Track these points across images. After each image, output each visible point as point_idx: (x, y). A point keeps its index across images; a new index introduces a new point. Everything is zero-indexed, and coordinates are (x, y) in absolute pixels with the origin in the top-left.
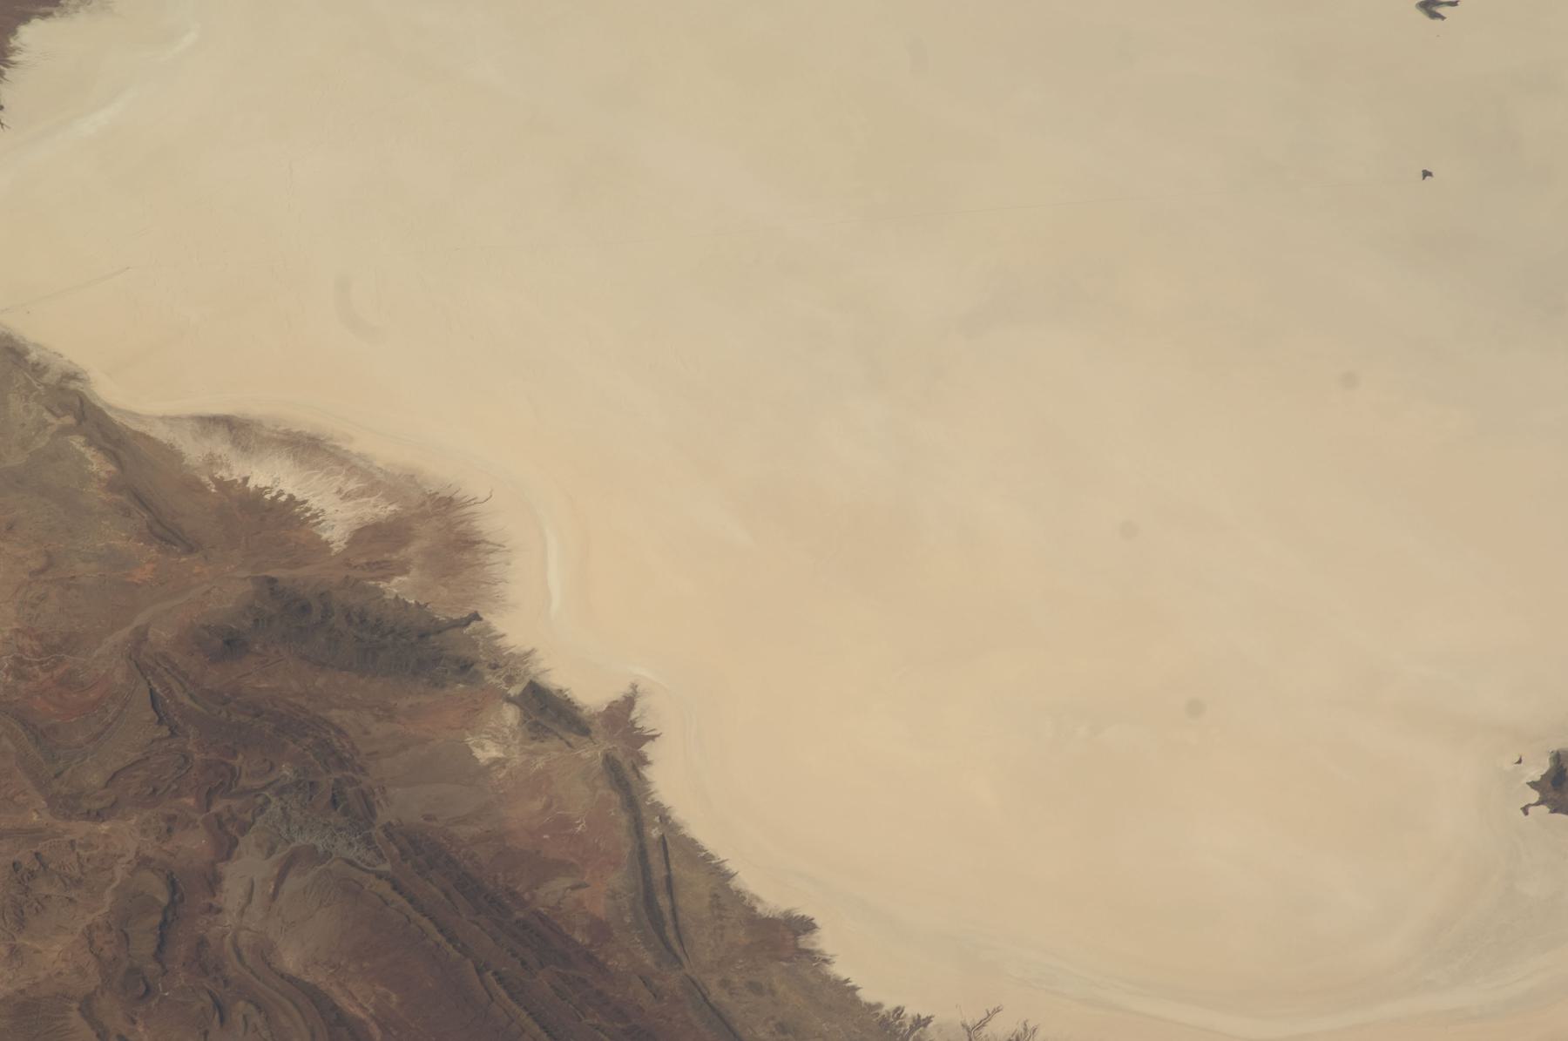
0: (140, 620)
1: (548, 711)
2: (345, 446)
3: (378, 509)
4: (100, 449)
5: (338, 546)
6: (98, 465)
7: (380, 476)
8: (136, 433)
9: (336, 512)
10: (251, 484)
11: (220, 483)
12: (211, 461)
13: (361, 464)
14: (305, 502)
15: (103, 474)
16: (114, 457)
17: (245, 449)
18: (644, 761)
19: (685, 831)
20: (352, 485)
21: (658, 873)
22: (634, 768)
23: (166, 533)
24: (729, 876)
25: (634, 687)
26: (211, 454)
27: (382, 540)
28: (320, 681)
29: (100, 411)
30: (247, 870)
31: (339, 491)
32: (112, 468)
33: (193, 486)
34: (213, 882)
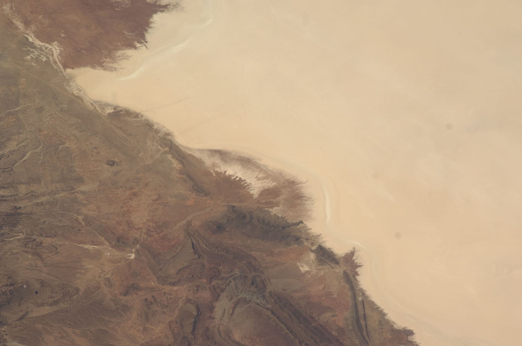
0: (189, 218)
1: (325, 255)
2: (259, 162)
3: (269, 184)
4: (177, 159)
5: (256, 196)
6: (176, 165)
7: (270, 173)
9: (255, 185)
10: (227, 174)
11: (217, 173)
12: (214, 165)
13: (264, 168)
14: (245, 180)
15: (178, 168)
16: (182, 162)
17: (225, 162)
18: (357, 274)
19: (370, 299)
20: (261, 175)
21: (361, 313)
22: (354, 276)
23: (198, 189)
24: (385, 315)
25: (354, 248)
26: (214, 163)
27: (270, 195)
28: (249, 242)
29: (177, 146)
30: (223, 305)
31: (256, 177)
32: (181, 166)
33: (207, 173)
34: (212, 309)
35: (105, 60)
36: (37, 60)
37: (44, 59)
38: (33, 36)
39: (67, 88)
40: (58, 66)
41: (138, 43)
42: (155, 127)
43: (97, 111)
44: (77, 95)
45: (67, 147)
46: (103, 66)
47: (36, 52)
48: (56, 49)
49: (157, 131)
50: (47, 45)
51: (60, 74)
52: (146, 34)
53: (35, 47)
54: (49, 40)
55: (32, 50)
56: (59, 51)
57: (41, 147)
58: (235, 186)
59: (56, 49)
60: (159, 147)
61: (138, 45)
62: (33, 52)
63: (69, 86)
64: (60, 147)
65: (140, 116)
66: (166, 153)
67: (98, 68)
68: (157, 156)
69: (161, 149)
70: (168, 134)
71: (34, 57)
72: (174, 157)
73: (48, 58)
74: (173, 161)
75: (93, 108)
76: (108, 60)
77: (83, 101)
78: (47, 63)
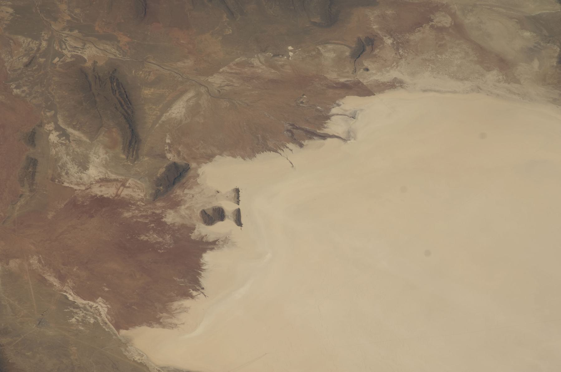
35: (161, 315)
36: (84, 322)
37: (92, 321)
38: (72, 294)
40: (109, 328)
41: (193, 290)
46: (160, 323)
47: (81, 312)
48: (102, 307)
50: (91, 303)
51: (114, 337)
52: (200, 279)
53: (77, 307)
54: (92, 297)
55: (75, 310)
56: (106, 310)
59: (102, 307)
61: (194, 293)
62: (76, 313)
67: (155, 325)
71: (80, 319)
73: (95, 318)
76: (165, 314)
78: (96, 324)
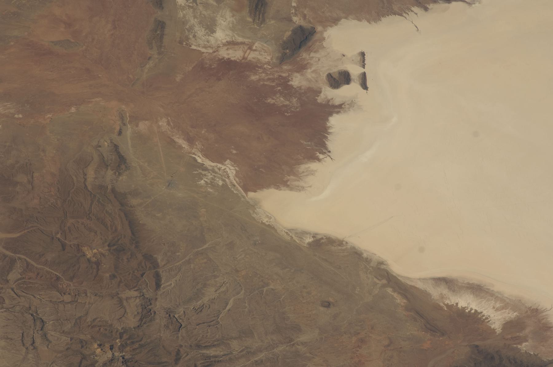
2: (492, 289)
3: (511, 315)
4: (399, 293)
5: (499, 330)
6: (399, 300)
7: (508, 301)
8: (411, 286)
10: (459, 306)
11: (447, 305)
12: (442, 297)
13: (499, 296)
14: (482, 312)
15: (402, 304)
16: (405, 297)
17: (454, 291)
20: (498, 305)
23: (431, 327)
26: (441, 294)
29: (395, 277)
31: (494, 308)
32: (405, 301)
33: (437, 308)
35: (289, 177)
36: (212, 184)
37: (221, 183)
38: (201, 156)
39: (254, 215)
40: (237, 190)
41: (320, 153)
42: (365, 255)
43: (295, 241)
44: (267, 224)
45: (272, 289)
46: (288, 186)
47: (209, 174)
48: (230, 169)
49: (368, 261)
50: (219, 165)
51: (242, 199)
52: (327, 142)
53: (206, 169)
54: (220, 158)
55: (203, 173)
56: (234, 172)
57: (243, 292)
58: (471, 321)
59: (230, 169)
60: (375, 279)
61: (321, 156)
62: (205, 175)
63: (256, 213)
64: (265, 289)
65: (344, 243)
66: (384, 286)
67: (282, 188)
68: (376, 291)
69: (378, 281)
70: (382, 263)
71: (209, 181)
72: (394, 291)
74: (395, 295)
75: (289, 238)
76: (292, 177)
77: (276, 230)
78: (225, 186)
